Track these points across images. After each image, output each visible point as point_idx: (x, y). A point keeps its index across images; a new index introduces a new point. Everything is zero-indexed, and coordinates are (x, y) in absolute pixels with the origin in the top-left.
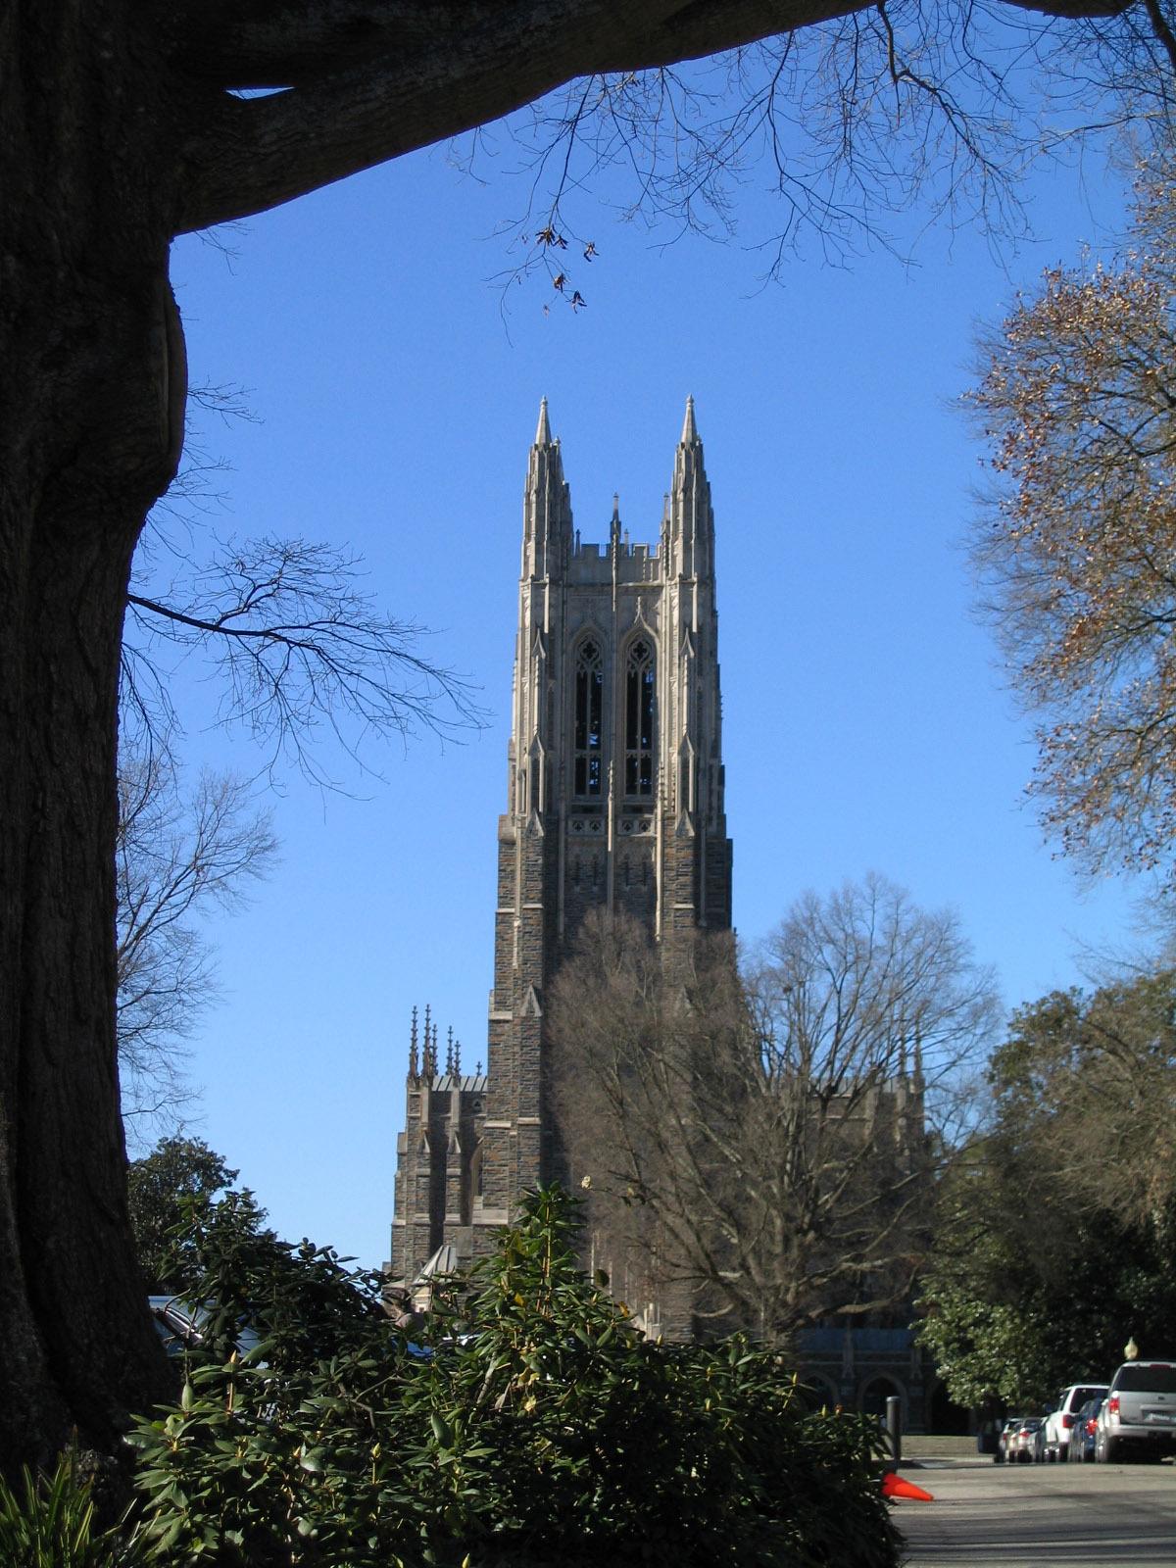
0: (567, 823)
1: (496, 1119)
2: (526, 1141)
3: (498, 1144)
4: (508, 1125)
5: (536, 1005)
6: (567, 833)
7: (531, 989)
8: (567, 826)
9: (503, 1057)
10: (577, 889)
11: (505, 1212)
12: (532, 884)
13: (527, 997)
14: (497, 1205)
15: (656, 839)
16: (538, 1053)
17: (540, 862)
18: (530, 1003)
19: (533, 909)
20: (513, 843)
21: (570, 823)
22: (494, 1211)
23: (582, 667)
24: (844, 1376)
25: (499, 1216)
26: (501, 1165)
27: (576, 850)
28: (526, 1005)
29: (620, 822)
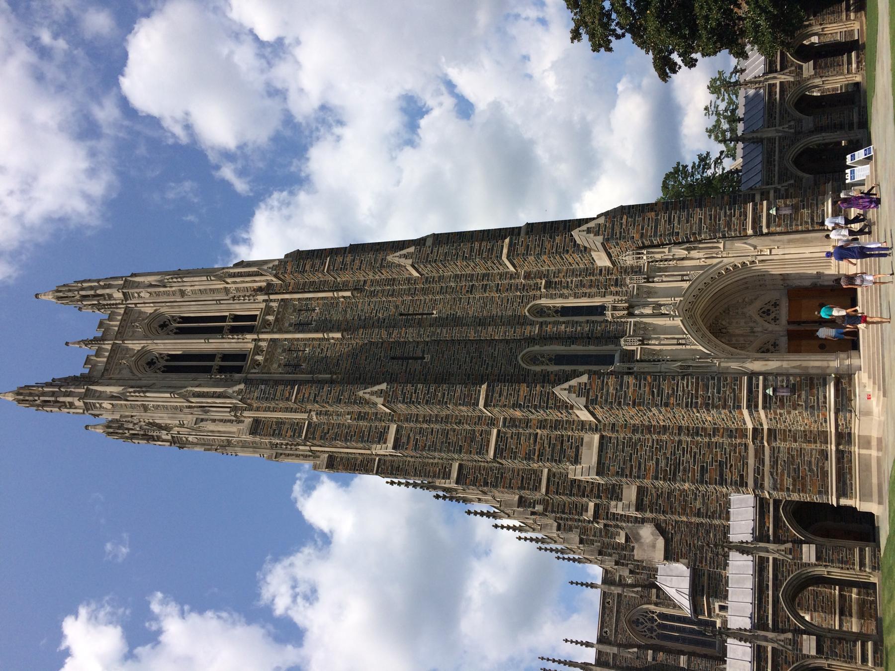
0: (252, 373)
1: (488, 445)
2: (503, 398)
3: (512, 443)
4: (495, 431)
5: (376, 388)
6: (258, 373)
7: (361, 393)
8: (255, 373)
9: (430, 436)
10: (304, 366)
11: (587, 437)
12: (278, 394)
13: (367, 396)
14: (577, 449)
15: (282, 299)
16: (420, 386)
17: (263, 387)
18: (372, 393)
19: (298, 393)
20: (256, 422)
21: (253, 371)
22: (584, 451)
23: (159, 369)
24: (792, 131)
25: (590, 444)
26: (535, 441)
27: (275, 366)
28: (374, 399)
29: (263, 330)
